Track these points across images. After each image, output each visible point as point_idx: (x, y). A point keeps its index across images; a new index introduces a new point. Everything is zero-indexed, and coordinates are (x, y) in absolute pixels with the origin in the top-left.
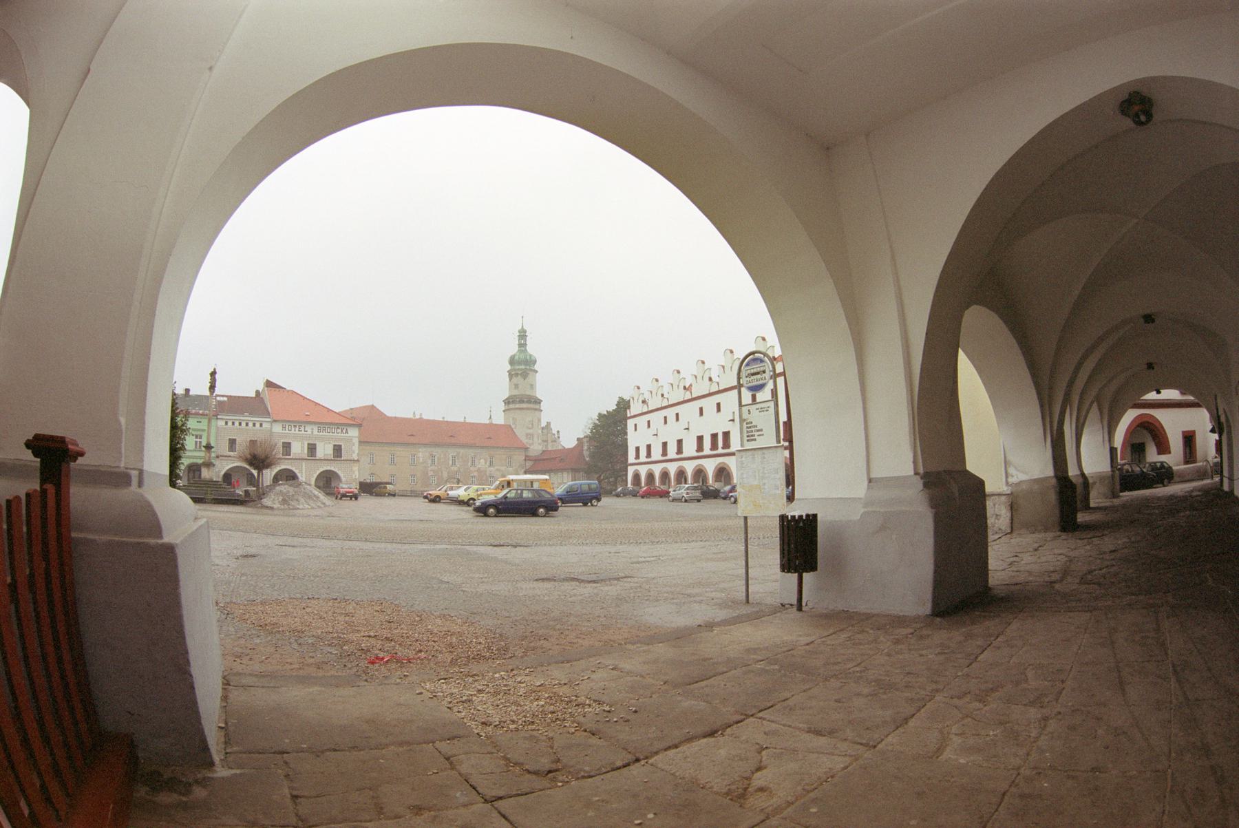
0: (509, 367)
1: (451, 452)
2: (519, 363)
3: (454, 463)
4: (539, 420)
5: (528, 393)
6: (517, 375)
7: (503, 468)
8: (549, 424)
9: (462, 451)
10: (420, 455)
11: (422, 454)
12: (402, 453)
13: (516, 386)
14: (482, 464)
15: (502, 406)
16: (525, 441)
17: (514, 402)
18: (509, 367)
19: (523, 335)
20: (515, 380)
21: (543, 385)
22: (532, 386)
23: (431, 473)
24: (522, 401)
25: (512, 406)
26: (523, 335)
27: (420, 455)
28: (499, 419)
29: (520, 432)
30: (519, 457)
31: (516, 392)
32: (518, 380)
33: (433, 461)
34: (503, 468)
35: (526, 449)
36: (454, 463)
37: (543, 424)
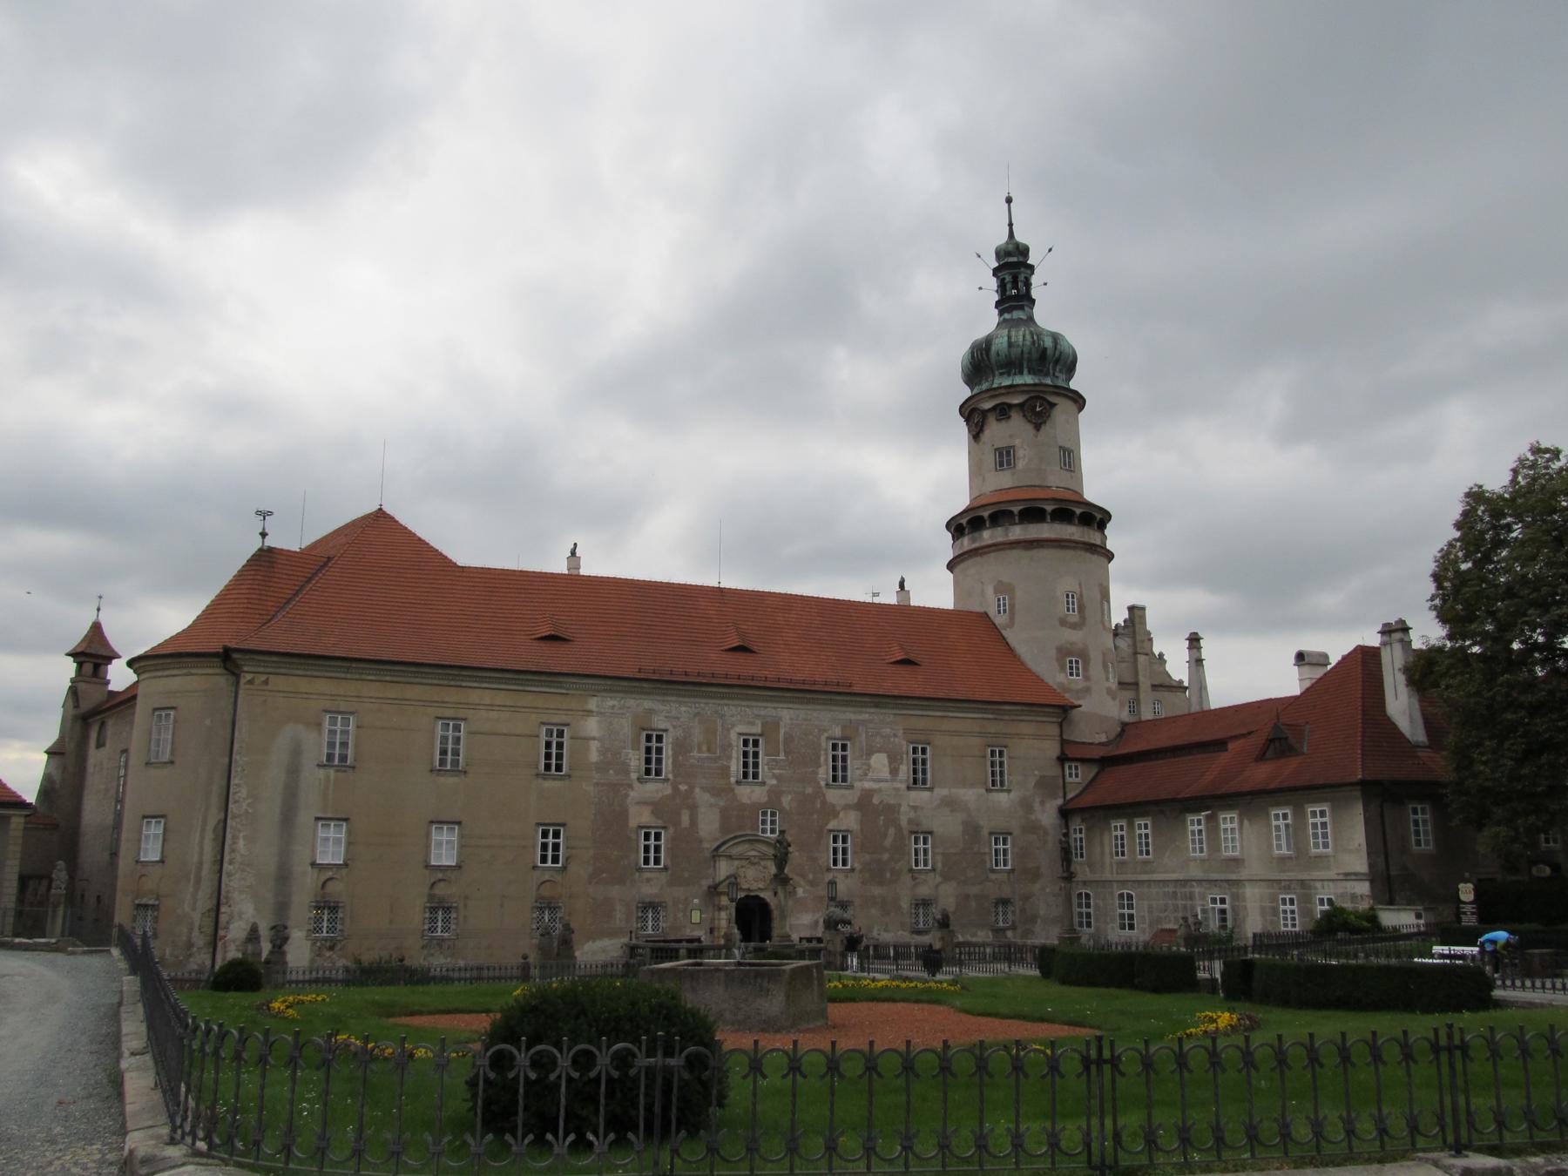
0: (966, 392)
1: (740, 720)
2: (1011, 365)
3: (750, 771)
4: (1105, 596)
5: (1056, 480)
6: (1003, 412)
7: (970, 795)
8: (1136, 613)
9: (788, 715)
10: (592, 726)
11: (600, 724)
12: (501, 721)
13: (1005, 457)
14: (877, 772)
15: (945, 546)
16: (1054, 676)
17: (1000, 516)
18: (966, 392)
19: (1013, 269)
20: (996, 432)
21: (1109, 461)
22: (1069, 459)
23: (640, 816)
24: (1032, 514)
25: (987, 536)
26: (1013, 269)
27: (592, 726)
28: (935, 590)
29: (1033, 646)
30: (1034, 748)
31: (1005, 480)
32: (1013, 432)
33: (652, 767)
34: (970, 795)
35: (1063, 711)
36: (750, 771)
37: (1118, 616)
